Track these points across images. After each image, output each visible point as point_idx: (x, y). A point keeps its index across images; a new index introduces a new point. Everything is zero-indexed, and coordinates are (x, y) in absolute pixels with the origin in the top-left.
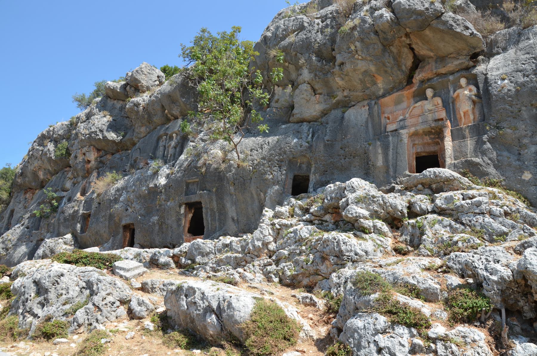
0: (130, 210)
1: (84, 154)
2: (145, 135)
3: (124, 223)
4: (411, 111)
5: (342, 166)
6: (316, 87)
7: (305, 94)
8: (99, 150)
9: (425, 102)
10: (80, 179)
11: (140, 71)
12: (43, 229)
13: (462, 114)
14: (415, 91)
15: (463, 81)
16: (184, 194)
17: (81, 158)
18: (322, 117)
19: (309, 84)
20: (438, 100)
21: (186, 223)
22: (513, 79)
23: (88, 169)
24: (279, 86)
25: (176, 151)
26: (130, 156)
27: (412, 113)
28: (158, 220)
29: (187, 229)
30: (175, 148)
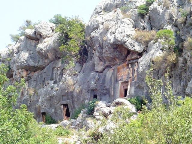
3: (42, 112)
8: (27, 70)
11: (41, 27)
17: (19, 75)
18: (103, 71)
19: (98, 57)
21: (64, 113)
28: (54, 111)
29: (65, 115)
30: (60, 75)
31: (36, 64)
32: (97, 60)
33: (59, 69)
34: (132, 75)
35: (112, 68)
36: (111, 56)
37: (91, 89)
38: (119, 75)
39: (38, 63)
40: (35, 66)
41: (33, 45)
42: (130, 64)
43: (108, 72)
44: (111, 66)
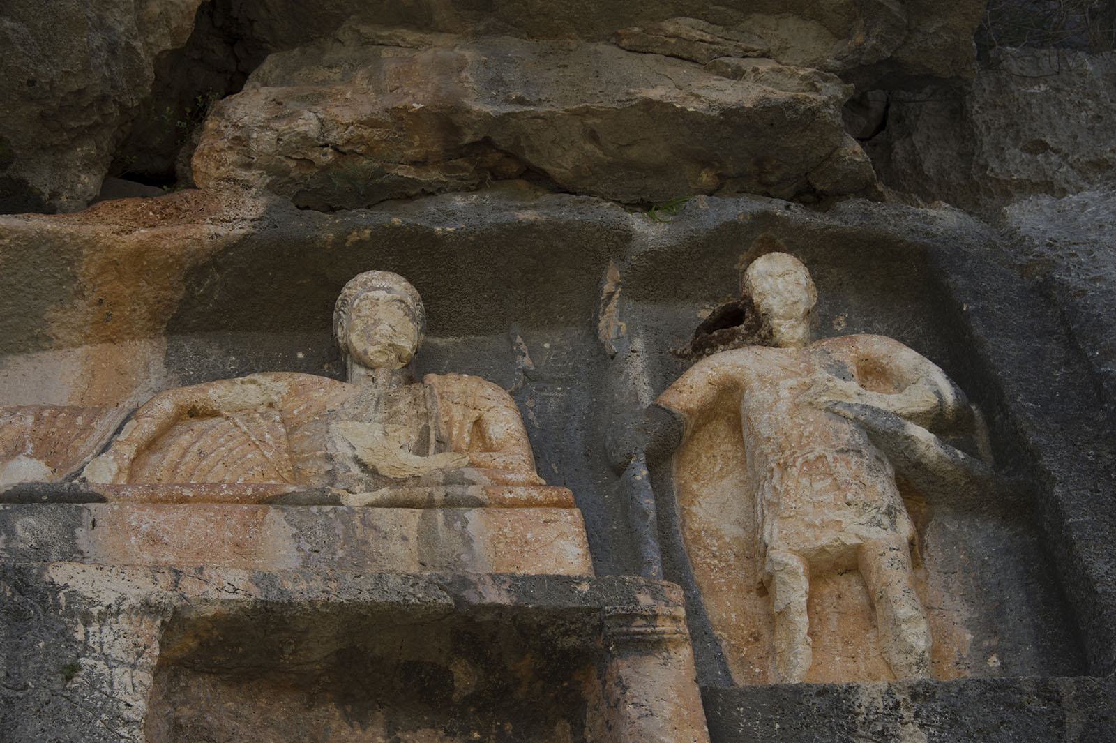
4: (151, 445)
9: (323, 391)
13: (795, 592)
14: (220, 258)
15: (779, 281)
27: (159, 466)
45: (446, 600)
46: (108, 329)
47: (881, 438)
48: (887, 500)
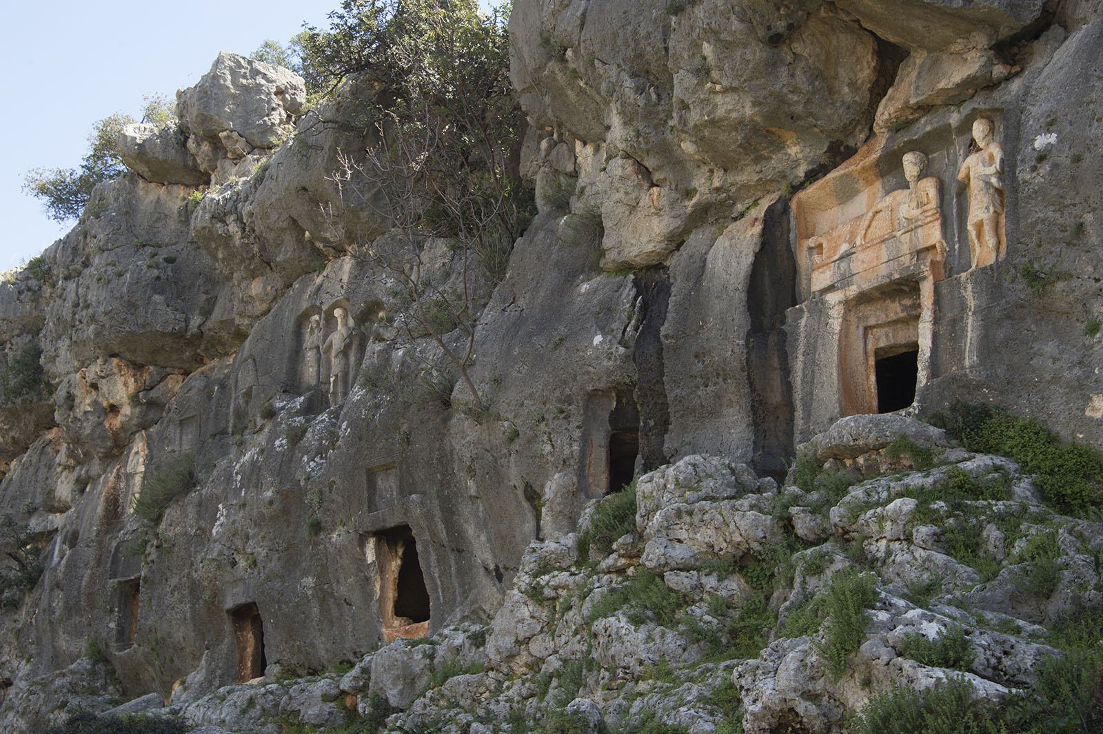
0: (242, 563)
1: (94, 386)
2: (264, 306)
3: (230, 603)
4: (869, 226)
5: (702, 406)
6: (650, 163)
7: (622, 191)
9: (901, 195)
10: (96, 467)
12: (6, 649)
14: (878, 163)
15: (978, 130)
16: (366, 508)
17: (88, 401)
19: (627, 156)
20: (929, 188)
21: (385, 588)
22: (1069, 128)
23: (116, 434)
24: (585, 144)
25: (347, 364)
26: (232, 382)
28: (318, 587)
29: (390, 606)
30: (344, 353)
31: (196, 321)
32: (622, 178)
33: (338, 312)
34: (945, 234)
35: (742, 215)
36: (749, 111)
37: (590, 388)
38: (817, 258)
39: (207, 313)
40: (189, 335)
41: (175, 216)
42: (911, 146)
43: (722, 243)
44: (740, 207)
45: (888, 280)
46: (869, 183)
47: (988, 184)
48: (985, 205)
